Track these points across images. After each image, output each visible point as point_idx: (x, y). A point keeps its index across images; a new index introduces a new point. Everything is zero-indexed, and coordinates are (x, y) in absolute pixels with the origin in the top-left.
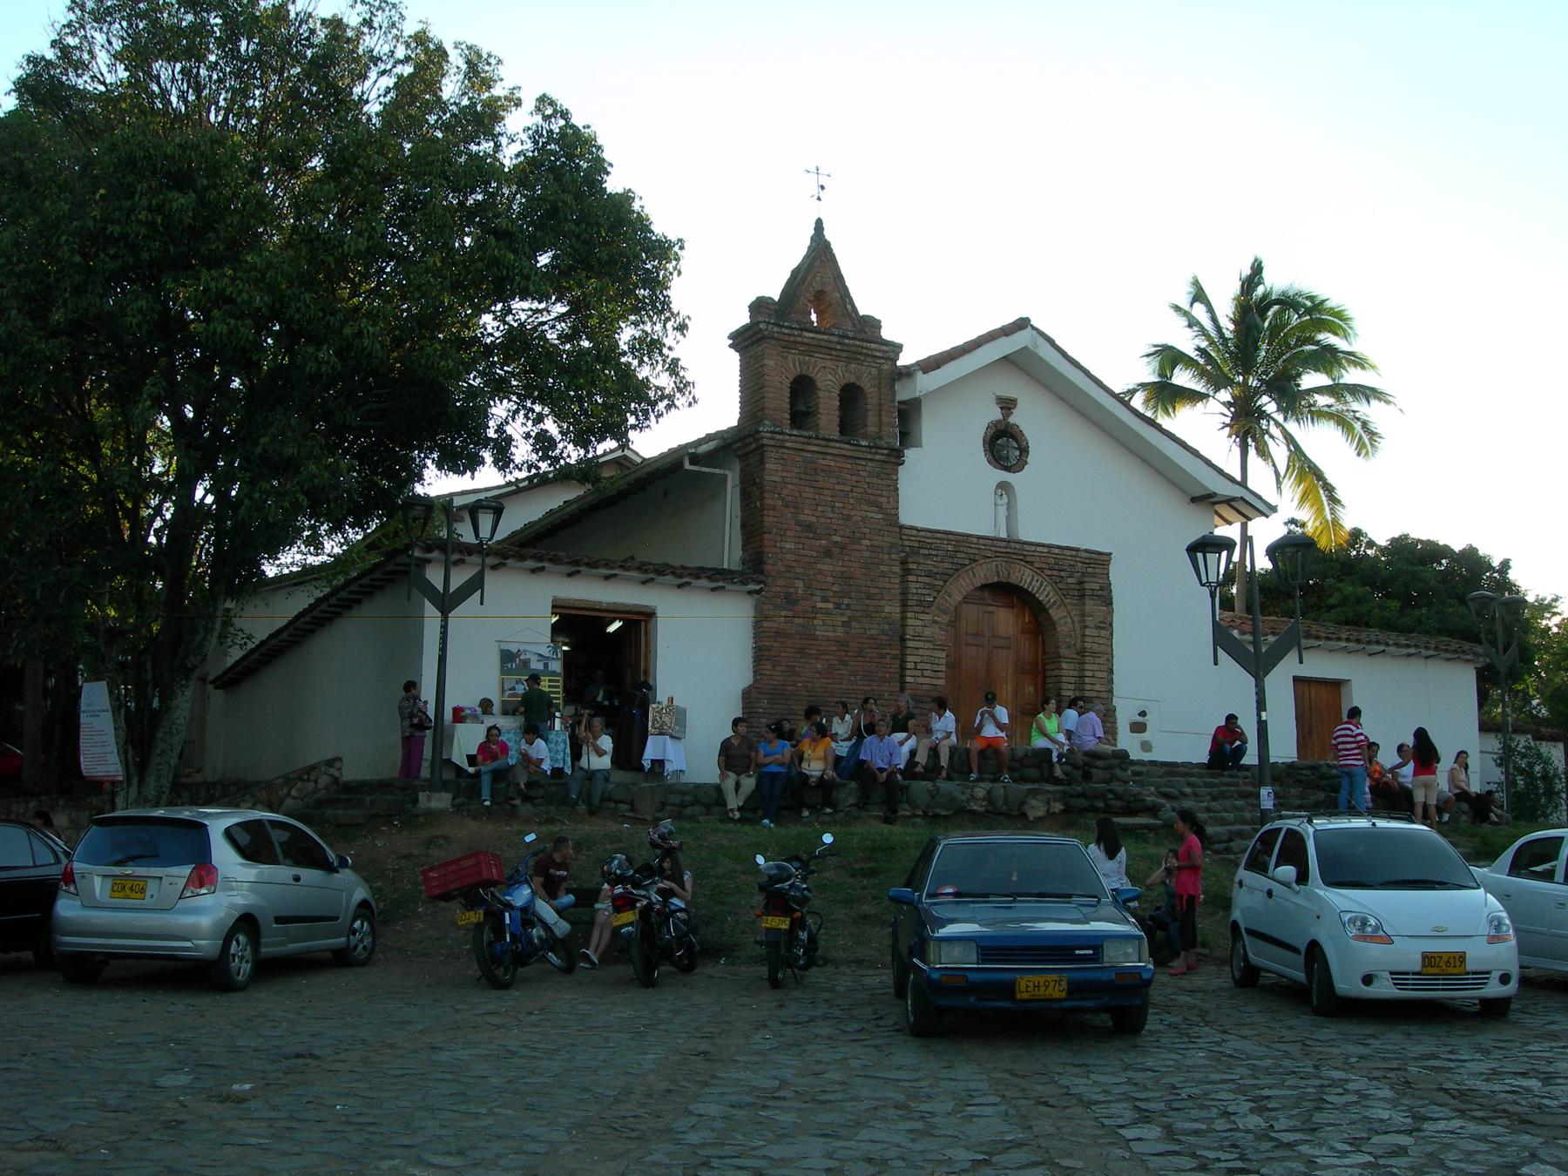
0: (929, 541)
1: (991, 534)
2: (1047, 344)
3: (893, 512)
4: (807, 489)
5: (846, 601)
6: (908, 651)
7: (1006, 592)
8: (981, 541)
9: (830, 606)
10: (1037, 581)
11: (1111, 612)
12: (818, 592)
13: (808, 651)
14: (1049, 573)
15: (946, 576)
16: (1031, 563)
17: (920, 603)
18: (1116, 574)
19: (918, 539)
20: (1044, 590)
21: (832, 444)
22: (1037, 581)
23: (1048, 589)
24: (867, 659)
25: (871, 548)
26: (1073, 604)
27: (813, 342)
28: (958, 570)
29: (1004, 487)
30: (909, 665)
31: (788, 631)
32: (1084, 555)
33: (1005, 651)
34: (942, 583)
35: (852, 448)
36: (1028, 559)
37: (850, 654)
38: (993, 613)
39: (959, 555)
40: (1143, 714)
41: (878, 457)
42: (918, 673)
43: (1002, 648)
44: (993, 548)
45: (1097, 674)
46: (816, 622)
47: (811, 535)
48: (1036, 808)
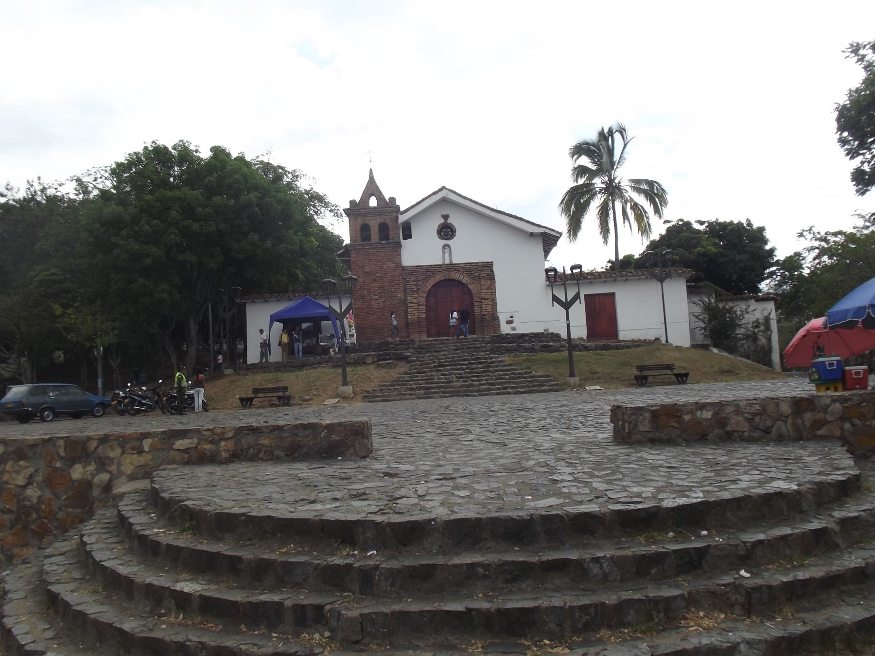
1: (440, 262)
2: (452, 193)
7: (450, 283)
15: (423, 281)
16: (459, 271)
17: (411, 291)
29: (448, 246)
40: (512, 317)
48: (369, 360)
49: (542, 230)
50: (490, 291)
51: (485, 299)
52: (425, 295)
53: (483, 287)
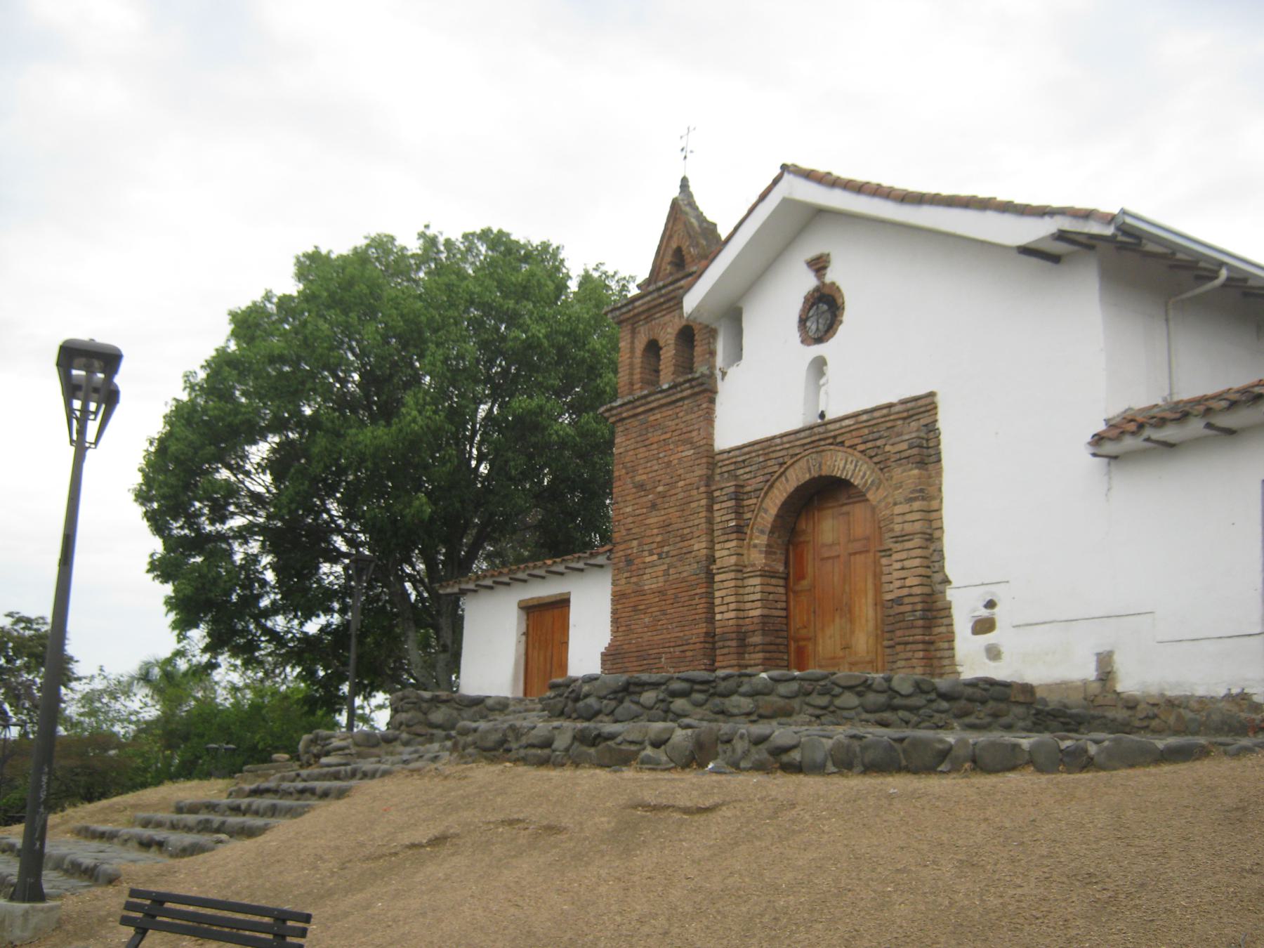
0: (740, 459)
3: (701, 443)
4: (641, 450)
5: (666, 549)
6: (716, 586)
8: (785, 439)
9: (655, 557)
11: (939, 473)
12: (646, 548)
13: (640, 607)
16: (842, 443)
18: (945, 421)
20: (860, 470)
21: (650, 399)
23: (865, 467)
24: (680, 604)
25: (685, 489)
27: (645, 307)
28: (767, 481)
30: (717, 601)
31: (627, 592)
35: (664, 395)
36: (839, 440)
37: (668, 602)
38: (848, 513)
40: (991, 604)
41: (685, 394)
42: (724, 608)
43: (860, 553)
44: (798, 443)
45: (908, 564)
46: (645, 577)
47: (643, 493)
49: (1048, 227)
50: (917, 505)
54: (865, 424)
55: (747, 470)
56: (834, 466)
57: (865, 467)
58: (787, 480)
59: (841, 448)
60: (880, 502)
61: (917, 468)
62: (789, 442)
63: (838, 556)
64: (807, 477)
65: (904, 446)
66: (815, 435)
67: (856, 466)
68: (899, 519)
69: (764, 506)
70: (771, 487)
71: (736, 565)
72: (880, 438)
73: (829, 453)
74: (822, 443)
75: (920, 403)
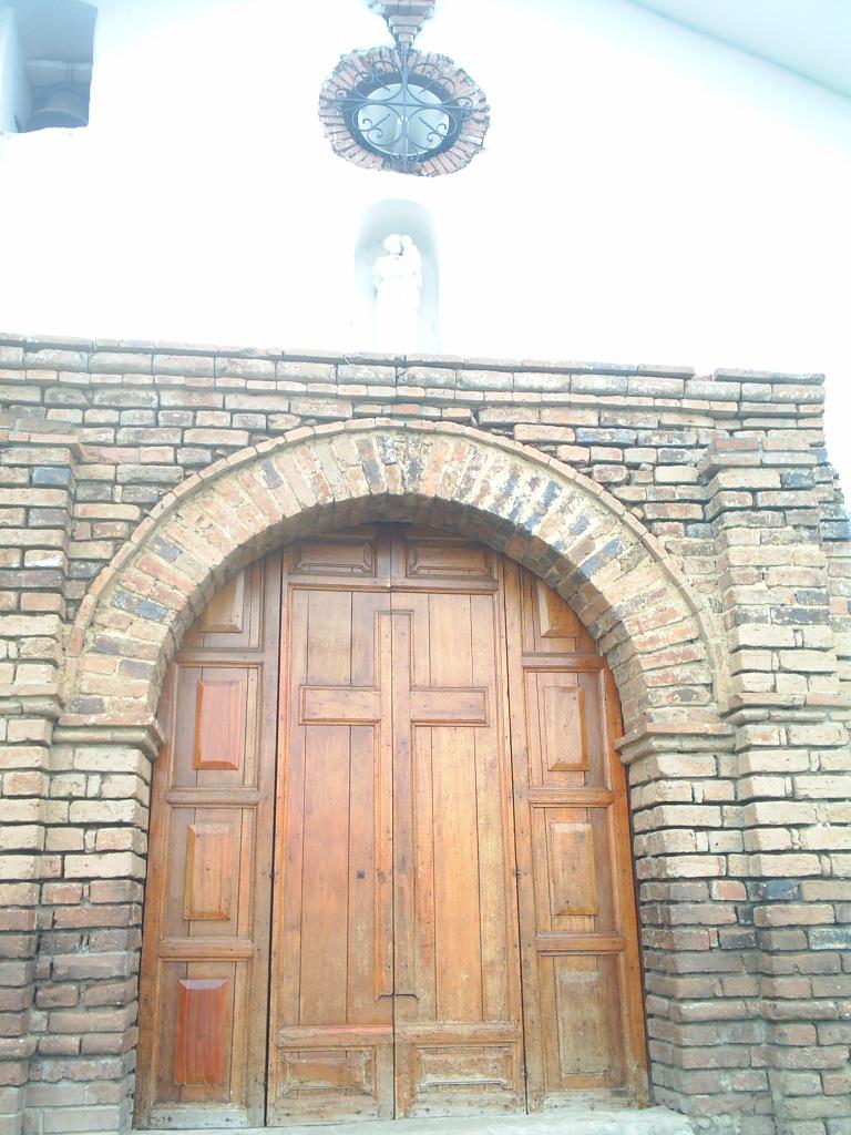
8: (291, 368)
10: (534, 483)
14: (581, 454)
15: (148, 492)
16: (507, 428)
19: (32, 375)
22: (534, 483)
26: (688, 551)
28: (202, 466)
32: (711, 388)
33: (464, 734)
34: (133, 513)
36: (485, 417)
38: (409, 613)
39: (204, 418)
45: (806, 785)
50: (816, 634)
51: (787, 713)
52: (155, 634)
53: (745, 594)
54: (593, 399)
55: (112, 416)
56: (468, 480)
57: (582, 505)
58: (274, 480)
59: (503, 441)
60: (636, 602)
61: (812, 539)
62: (305, 381)
63: (375, 723)
64: (362, 488)
65: (771, 478)
66: (412, 384)
67: (551, 496)
68: (764, 660)
69: (172, 532)
70: (205, 486)
71: (56, 698)
72: (636, 444)
73: (452, 443)
74: (434, 412)
75: (782, 391)
